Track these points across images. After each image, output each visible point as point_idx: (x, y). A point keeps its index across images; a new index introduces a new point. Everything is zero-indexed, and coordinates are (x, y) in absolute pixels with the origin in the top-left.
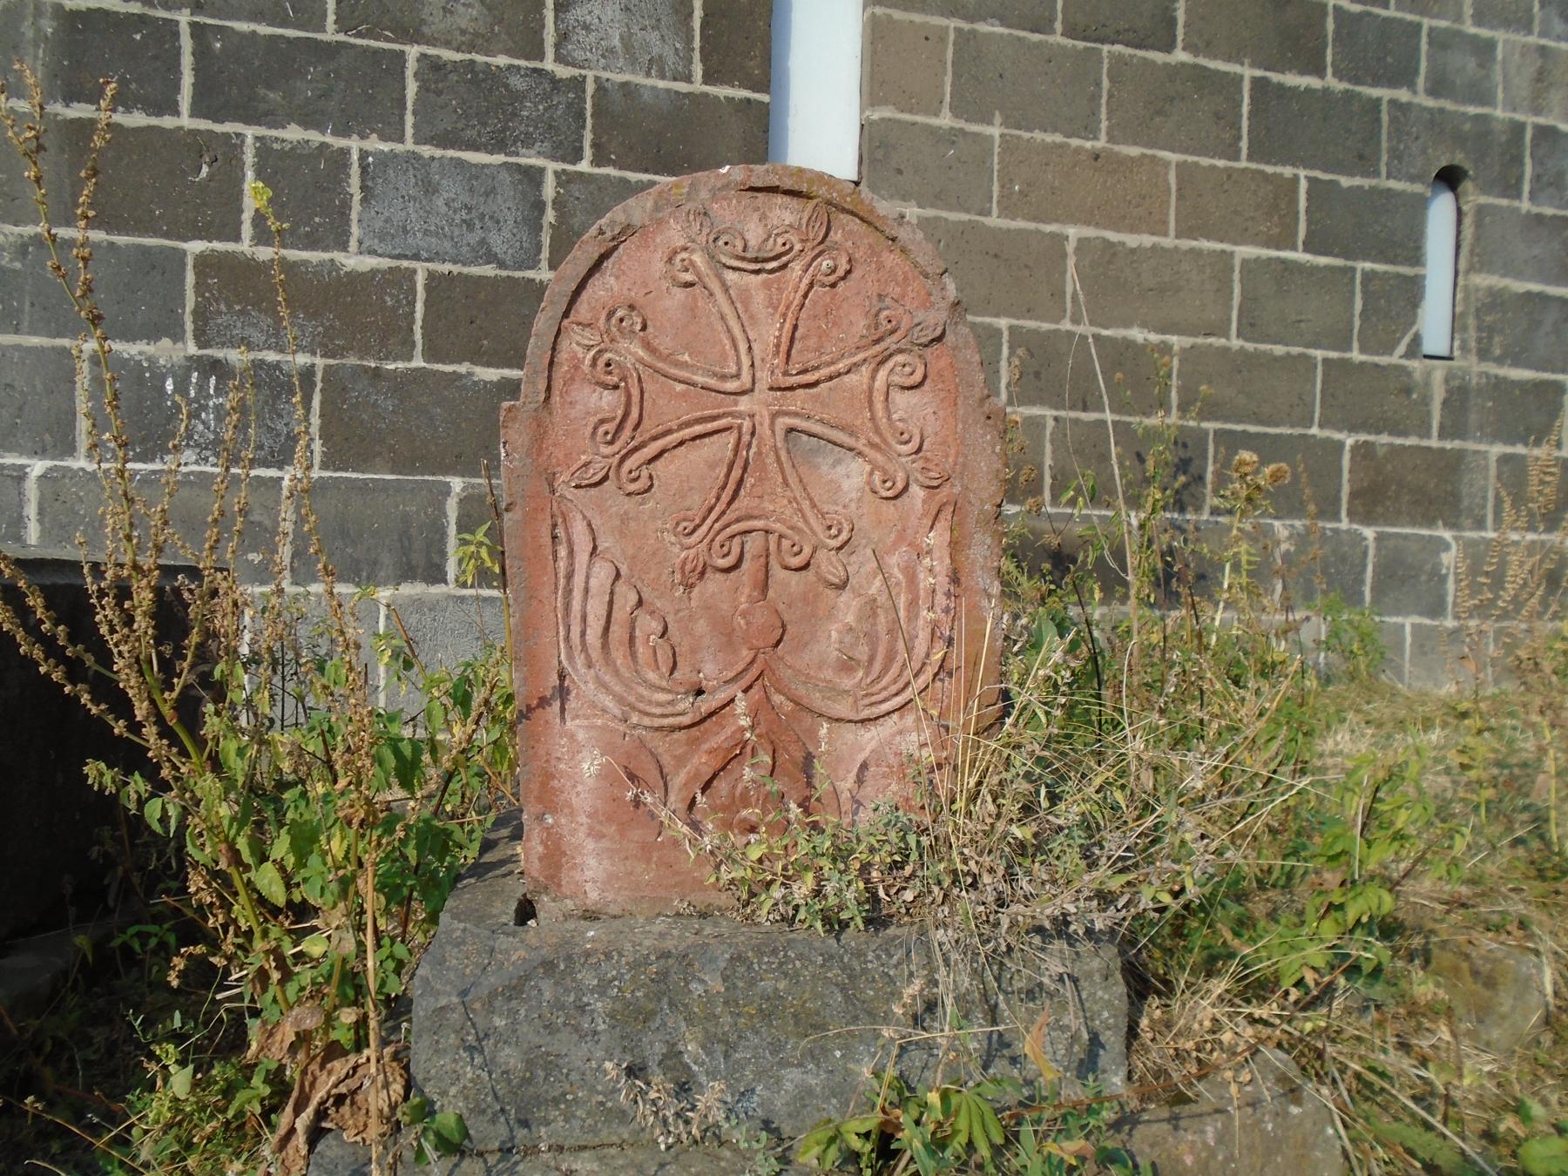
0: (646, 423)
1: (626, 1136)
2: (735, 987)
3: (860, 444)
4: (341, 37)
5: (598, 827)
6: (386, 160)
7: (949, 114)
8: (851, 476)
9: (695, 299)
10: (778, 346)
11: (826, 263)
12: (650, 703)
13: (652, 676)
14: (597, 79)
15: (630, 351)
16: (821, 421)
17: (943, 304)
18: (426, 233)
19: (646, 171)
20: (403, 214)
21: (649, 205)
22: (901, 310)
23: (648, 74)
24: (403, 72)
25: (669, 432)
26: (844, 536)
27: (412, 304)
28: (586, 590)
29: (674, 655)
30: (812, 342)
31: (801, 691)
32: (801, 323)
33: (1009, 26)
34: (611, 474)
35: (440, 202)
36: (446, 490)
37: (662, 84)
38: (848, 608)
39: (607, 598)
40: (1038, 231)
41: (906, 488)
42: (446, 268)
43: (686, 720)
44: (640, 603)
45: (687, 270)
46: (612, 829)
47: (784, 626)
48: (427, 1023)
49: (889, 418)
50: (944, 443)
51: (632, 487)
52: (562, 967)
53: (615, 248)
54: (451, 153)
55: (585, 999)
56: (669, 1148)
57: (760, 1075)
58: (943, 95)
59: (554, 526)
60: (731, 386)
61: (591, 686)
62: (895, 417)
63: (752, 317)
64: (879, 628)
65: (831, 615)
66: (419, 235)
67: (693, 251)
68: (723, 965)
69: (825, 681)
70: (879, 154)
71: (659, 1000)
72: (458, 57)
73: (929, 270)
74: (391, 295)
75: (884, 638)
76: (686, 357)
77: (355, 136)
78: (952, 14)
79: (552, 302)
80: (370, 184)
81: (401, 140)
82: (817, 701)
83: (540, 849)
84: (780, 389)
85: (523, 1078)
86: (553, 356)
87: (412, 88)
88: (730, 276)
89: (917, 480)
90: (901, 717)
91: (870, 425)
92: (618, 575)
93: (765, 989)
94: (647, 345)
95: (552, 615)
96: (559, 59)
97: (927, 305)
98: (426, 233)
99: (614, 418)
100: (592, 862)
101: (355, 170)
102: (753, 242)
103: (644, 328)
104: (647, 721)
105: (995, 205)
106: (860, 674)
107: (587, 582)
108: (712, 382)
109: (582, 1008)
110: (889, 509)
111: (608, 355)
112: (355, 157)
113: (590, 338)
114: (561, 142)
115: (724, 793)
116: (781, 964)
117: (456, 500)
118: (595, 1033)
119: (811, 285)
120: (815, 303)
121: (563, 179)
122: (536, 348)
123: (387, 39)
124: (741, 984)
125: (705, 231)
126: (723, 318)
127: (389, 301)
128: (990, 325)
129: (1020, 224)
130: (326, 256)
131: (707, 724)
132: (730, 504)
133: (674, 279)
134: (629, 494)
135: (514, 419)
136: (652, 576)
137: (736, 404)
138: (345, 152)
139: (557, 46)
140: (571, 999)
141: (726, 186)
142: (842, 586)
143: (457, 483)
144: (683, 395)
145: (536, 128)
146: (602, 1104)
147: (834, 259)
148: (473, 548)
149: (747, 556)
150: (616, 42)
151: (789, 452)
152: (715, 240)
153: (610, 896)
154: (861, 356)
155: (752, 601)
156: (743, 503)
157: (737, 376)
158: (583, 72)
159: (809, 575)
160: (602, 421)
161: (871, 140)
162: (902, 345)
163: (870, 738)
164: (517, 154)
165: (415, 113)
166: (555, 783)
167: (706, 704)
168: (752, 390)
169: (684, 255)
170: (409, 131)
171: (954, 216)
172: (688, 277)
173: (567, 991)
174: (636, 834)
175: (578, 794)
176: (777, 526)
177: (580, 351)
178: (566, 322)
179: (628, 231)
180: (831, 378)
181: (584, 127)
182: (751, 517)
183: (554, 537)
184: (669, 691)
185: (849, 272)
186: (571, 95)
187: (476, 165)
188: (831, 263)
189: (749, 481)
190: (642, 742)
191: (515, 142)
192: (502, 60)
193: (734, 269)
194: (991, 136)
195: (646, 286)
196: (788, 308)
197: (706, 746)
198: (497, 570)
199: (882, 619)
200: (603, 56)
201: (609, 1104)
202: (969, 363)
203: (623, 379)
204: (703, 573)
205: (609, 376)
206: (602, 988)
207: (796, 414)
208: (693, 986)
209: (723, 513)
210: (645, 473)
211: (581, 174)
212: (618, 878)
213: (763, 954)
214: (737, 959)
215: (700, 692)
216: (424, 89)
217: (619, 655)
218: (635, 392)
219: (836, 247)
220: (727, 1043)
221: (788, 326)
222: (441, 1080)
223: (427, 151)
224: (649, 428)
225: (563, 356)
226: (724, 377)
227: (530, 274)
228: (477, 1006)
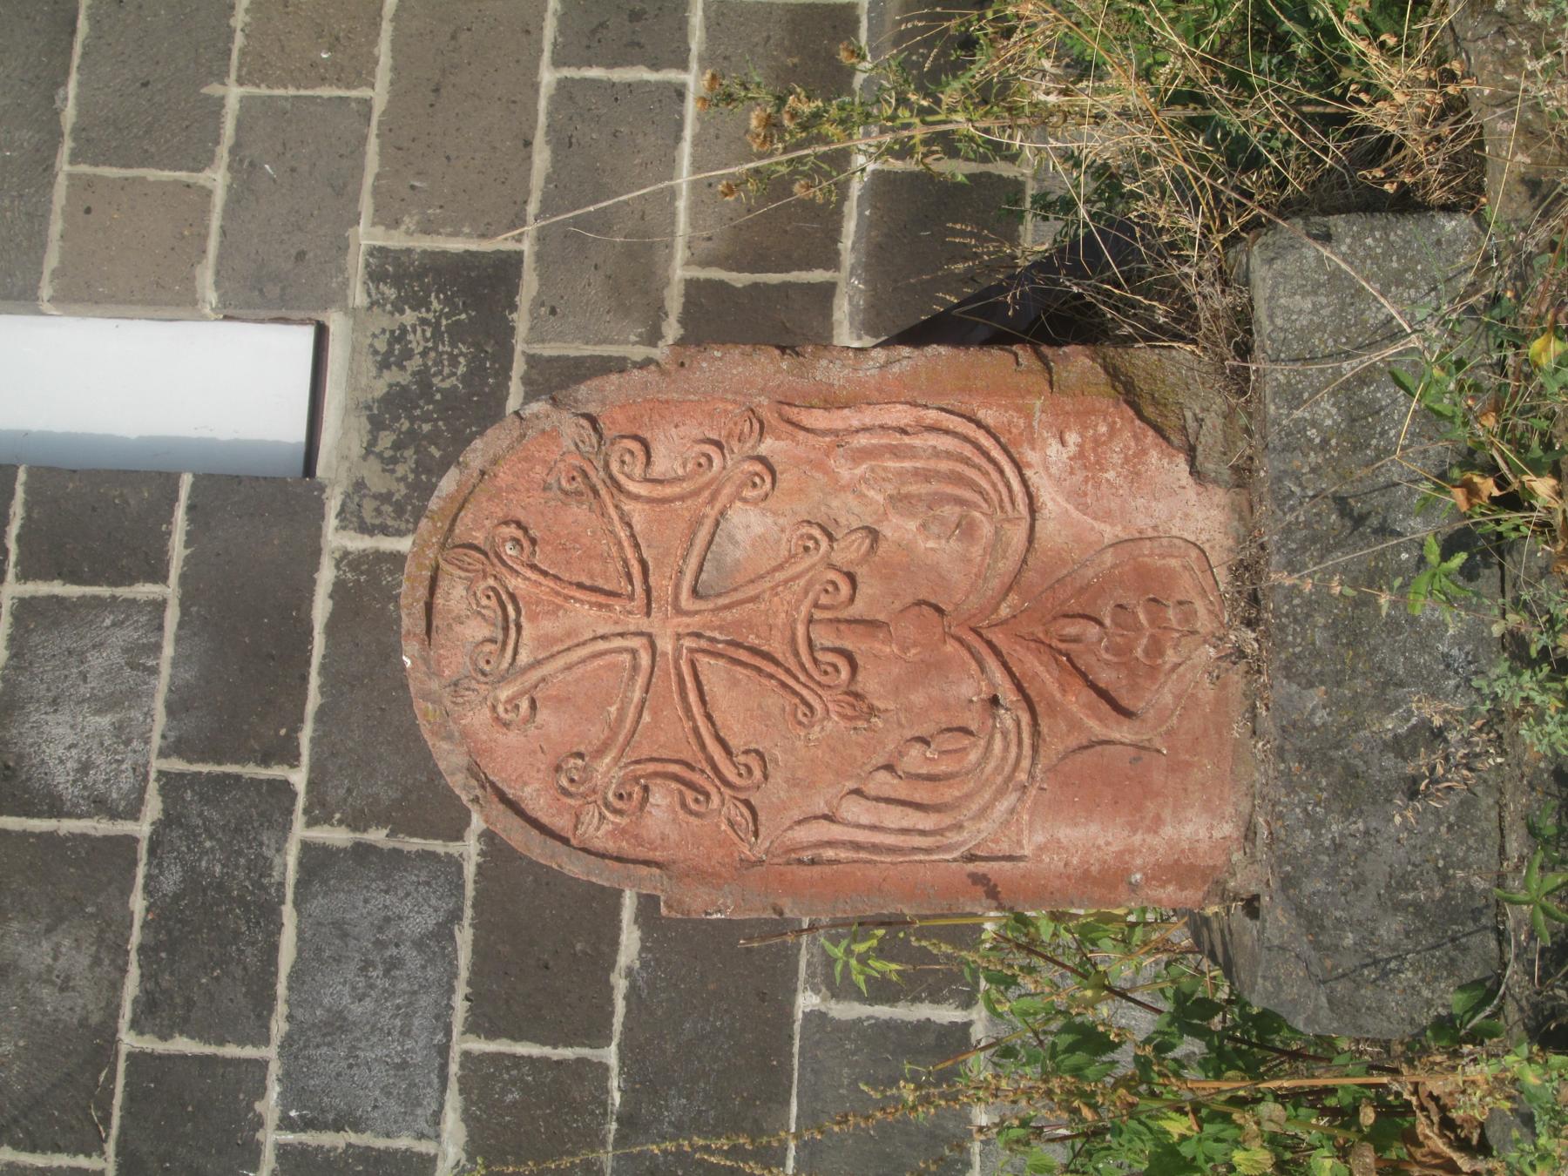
0: (684, 756)
1: (1491, 801)
2: (1321, 673)
3: (712, 512)
4: (110, 1147)
5: (1147, 822)
6: (294, 1091)
7: (208, 173)
8: (749, 525)
9: (548, 698)
10: (600, 606)
11: (509, 550)
12: (1004, 759)
13: (973, 756)
14: (163, 754)
16: (684, 558)
17: (555, 416)
18: (406, 1033)
19: (305, 679)
20: (376, 1068)
21: (445, 746)
22: (561, 465)
23: (154, 671)
24: (160, 1057)
25: (696, 730)
26: (817, 533)
27: (517, 1060)
28: (873, 828)
29: (949, 730)
30: (597, 567)
31: (995, 583)
32: (575, 579)
33: (67, 73)
34: (742, 796)
35: (357, 1009)
36: (816, 1019)
37: (168, 650)
38: (900, 528)
39: (883, 805)
40: (396, 18)
41: (762, 460)
42: (460, 1005)
43: (1025, 718)
44: (889, 768)
45: (517, 707)
46: (1151, 806)
47: (920, 603)
48: (1347, 1019)
49: (680, 479)
50: (711, 415)
51: (757, 773)
52: (1289, 868)
53: (493, 785)
54: (281, 989)
55: (1327, 843)
56: (1503, 753)
57: (1424, 646)
58: (176, 182)
59: (800, 862)
60: (645, 659)
61: (983, 825)
62: (680, 472)
63: (569, 635)
64: (923, 491)
65: (906, 548)
66: (409, 1044)
67: (496, 699)
68: (1294, 687)
69: (984, 555)
70: (273, 291)
71: (1332, 760)
72: (134, 972)
73: (516, 434)
74: (504, 1092)
75: (935, 486)
76: (613, 709)
77: (259, 1135)
78: (49, 168)
79: (552, 857)
80: (331, 1117)
81: (263, 1065)
82: (1007, 565)
83: (1171, 888)
84: (649, 604)
85: (1415, 914)
86: (611, 858)
88: (524, 657)
89: (753, 447)
90: (1030, 465)
91: (689, 502)
92: (857, 792)
93: (1325, 640)
94: (600, 752)
95: (900, 868)
96: (133, 813)
97: (553, 435)
98: (406, 1033)
99: (680, 792)
100: (1188, 830)
101: (310, 1138)
102: (484, 631)
103: (580, 755)
104: (1026, 763)
105: (353, 93)
106: (977, 514)
107: (863, 827)
108: (641, 680)
109: (1338, 847)
110: (786, 480)
111: (610, 797)
112: (289, 1137)
113: (591, 816)
114: (262, 814)
115: (1114, 675)
116: (1296, 621)
117: (832, 1004)
118: (1367, 833)
119: (533, 567)
120: (553, 564)
122: (602, 875)
123: (112, 1077)
124: (1318, 667)
125: (474, 685)
126: (569, 667)
127: (513, 1096)
128: (552, 100)
129: (384, 50)
131: (1032, 693)
132: (777, 663)
133: (526, 721)
134: (766, 777)
135: (680, 902)
136: (858, 753)
137: (665, 654)
138: (283, 1151)
139: (114, 815)
140: (1326, 859)
141: (426, 661)
142: (874, 534)
143: (807, 1001)
144: (655, 713)
145: (240, 853)
146: (1450, 827)
147: (504, 541)
148: (853, 962)
149: (838, 644)
150: (105, 721)
151: (719, 595)
152: (484, 674)
153: (1229, 810)
154: (612, 511)
155: (889, 639)
156: (777, 648)
157: (634, 652)
158: (153, 775)
159: (861, 572)
160: (684, 805)
161: (249, 305)
162: (600, 464)
163: (1052, 500)
164: (281, 884)
165: (221, 1042)
166: (1094, 869)
167: (1008, 695)
168: (650, 636)
169: (501, 709)
170: (249, 1052)
172: (524, 705)
173: (1316, 863)
174: (1158, 778)
175: (1108, 844)
176: (804, 609)
177: (606, 827)
178: (574, 842)
179: (474, 771)
180: (637, 546)
181: (238, 777)
182: (793, 640)
183: (813, 862)
184: (992, 737)
185: (519, 525)
186: (189, 795)
187: (300, 951)
188: (509, 545)
189: (752, 640)
190: (1051, 769)
191: (263, 888)
192: (138, 903)
193: (516, 652)
194: (242, 100)
195: (535, 752)
196: (558, 594)
197: (1058, 695)
198: (881, 932)
199: (913, 489)
200: (128, 742)
201: (1452, 819)
202: (620, 386)
203: (636, 779)
204: (857, 695)
205: (632, 796)
206: (1315, 824)
207: (677, 587)
208: (1317, 721)
209: (788, 671)
210: (742, 759)
211: (311, 783)
212: (1209, 800)
213: (1284, 642)
214: (1288, 670)
215: (994, 701)
217: (949, 793)
218: (651, 767)
219: (491, 539)
220: (1386, 684)
221: (578, 594)
222: (1414, 1006)
223: (279, 1026)
224: (690, 752)
225: (611, 846)
226: (635, 668)
227: (470, 871)
228: (1328, 963)
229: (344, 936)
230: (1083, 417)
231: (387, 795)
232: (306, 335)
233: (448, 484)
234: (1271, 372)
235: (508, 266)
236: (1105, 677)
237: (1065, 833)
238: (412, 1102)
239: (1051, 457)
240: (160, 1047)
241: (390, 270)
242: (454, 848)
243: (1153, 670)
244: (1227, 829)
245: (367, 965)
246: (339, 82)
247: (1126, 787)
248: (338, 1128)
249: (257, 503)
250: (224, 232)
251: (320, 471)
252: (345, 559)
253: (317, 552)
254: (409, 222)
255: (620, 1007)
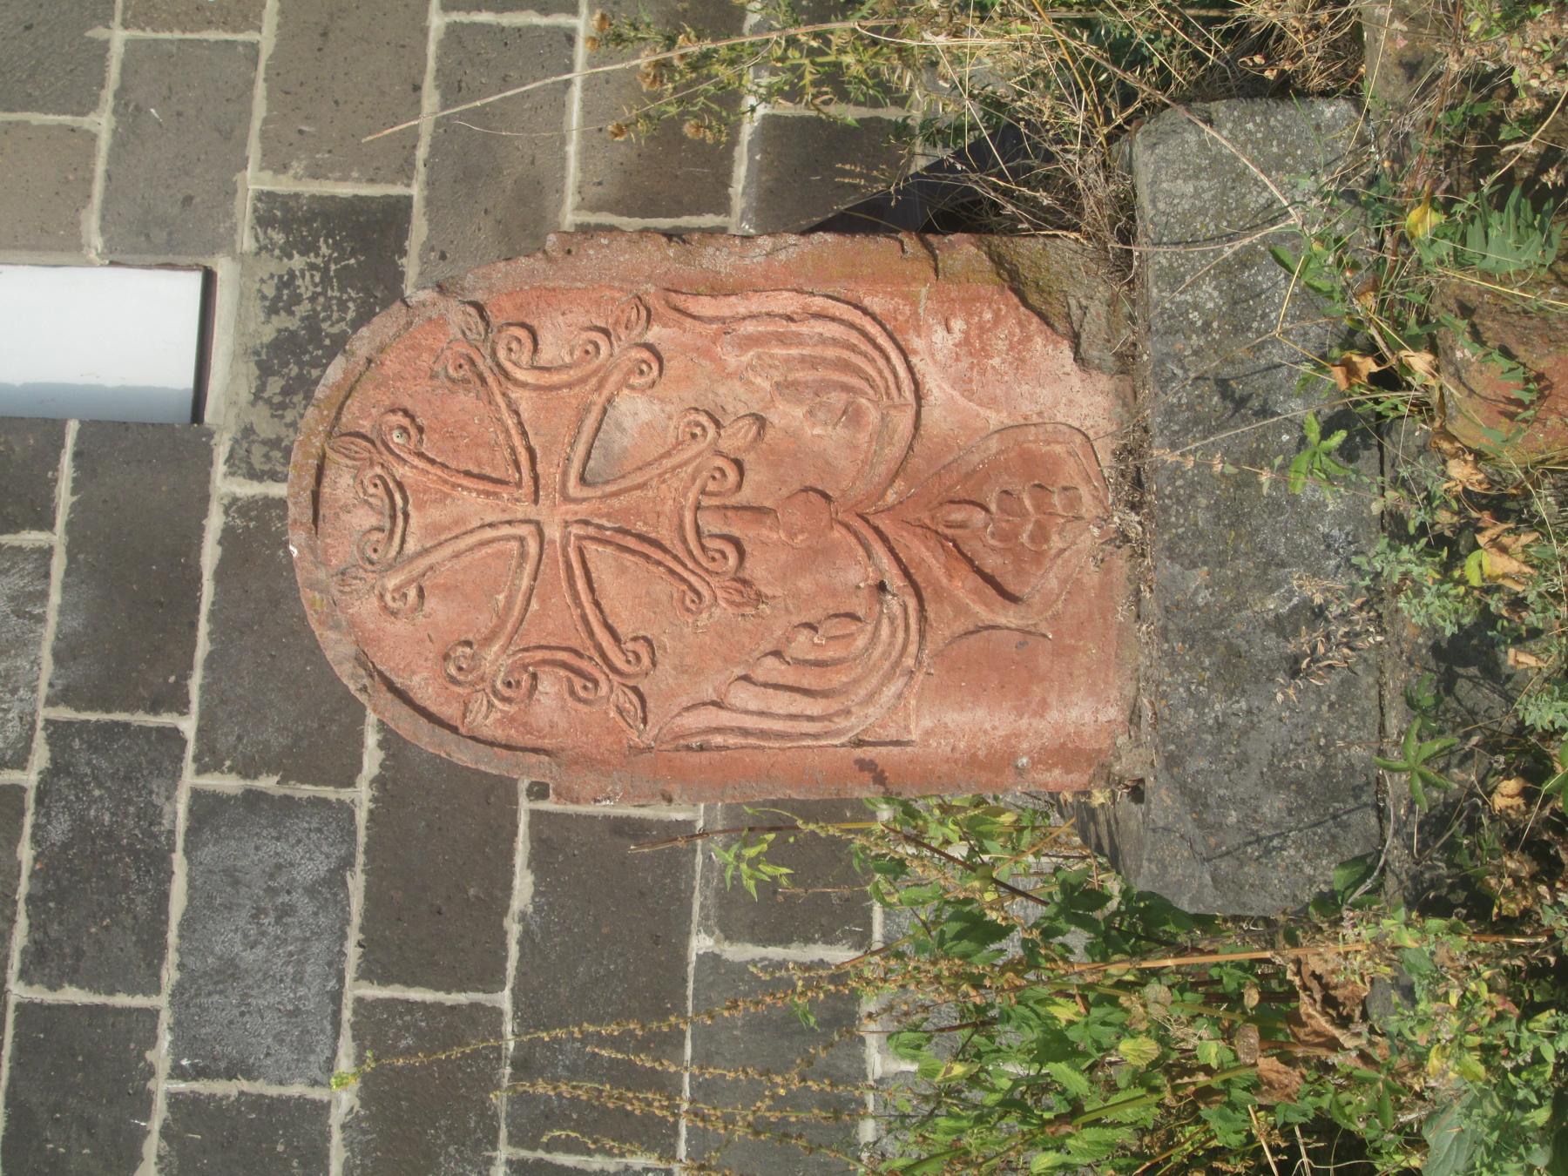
0: (574, 643)
1: (1371, 680)
2: (1203, 554)
3: (599, 400)
5: (1034, 706)
6: (185, 1040)
7: (92, 117)
8: (636, 412)
9: (437, 586)
10: (488, 494)
11: (396, 438)
12: (891, 644)
13: (861, 642)
14: (50, 702)
15: (494, 659)
16: (572, 445)
17: (441, 304)
18: (298, 979)
19: (193, 625)
20: (268, 1015)
21: (332, 635)
22: (448, 353)
23: (41, 619)
24: (50, 1007)
25: (584, 618)
26: (704, 419)
27: (410, 1006)
28: (761, 714)
29: (836, 616)
30: (484, 454)
31: (882, 469)
32: (463, 467)
34: (631, 683)
35: (249, 956)
36: (711, 961)
37: (55, 598)
38: (787, 415)
39: (771, 691)
41: (649, 347)
42: (353, 952)
43: (912, 604)
44: (777, 654)
45: (405, 595)
46: (1037, 690)
47: (806, 490)
48: (1231, 896)
49: (568, 367)
50: (598, 303)
51: (646, 660)
52: (1172, 747)
53: (381, 674)
54: (172, 937)
55: (1211, 722)
56: (1383, 632)
57: (1306, 528)
58: (60, 126)
59: (688, 748)
60: (533, 547)
61: (871, 710)
62: (568, 359)
63: (456, 523)
64: (810, 378)
65: (792, 435)
66: (302, 991)
67: (384, 588)
68: (1178, 567)
69: (870, 442)
70: (160, 236)
71: (1215, 640)
73: (402, 322)
74: (397, 1038)
75: (821, 373)
76: (501, 597)
77: (151, 1085)
79: (440, 745)
80: (223, 1065)
81: (153, 1014)
82: (894, 451)
83: (1057, 772)
84: (536, 492)
85: (1297, 792)
86: (500, 746)
87: (72, 995)
88: (412, 546)
89: (641, 335)
90: (915, 352)
91: (577, 390)
92: (746, 678)
93: (1207, 521)
94: (488, 641)
95: (788, 753)
96: (20, 762)
97: (440, 323)
98: (298, 979)
99: (569, 679)
100: (1074, 713)
101: (202, 1087)
102: (371, 520)
103: (469, 644)
104: (913, 649)
105: (240, 37)
106: (863, 401)
107: (752, 713)
108: (529, 568)
109: (1221, 726)
110: (674, 366)
111: (499, 685)
112: (181, 1086)
113: (479, 705)
114: (151, 762)
115: (1000, 561)
116: (1179, 502)
117: (726, 946)
118: (1249, 712)
119: (421, 455)
120: (441, 451)
121: (209, 760)
122: (491, 764)
124: (1201, 548)
125: (361, 573)
126: (457, 555)
128: (442, 44)
130: (337, 1137)
131: (919, 579)
132: (665, 550)
133: (414, 610)
134: (654, 664)
135: (569, 789)
136: (746, 640)
137: (553, 542)
138: (175, 1101)
140: (1210, 738)
141: (313, 550)
142: (761, 421)
143: (700, 943)
144: (543, 602)
145: (129, 802)
146: (1331, 706)
147: (391, 429)
148: (744, 866)
149: (726, 530)
151: (607, 482)
152: (371, 563)
153: (1114, 694)
154: (499, 399)
155: (776, 526)
156: (665, 535)
157: (521, 540)
158: (40, 724)
159: (749, 459)
160: (572, 693)
161: (135, 250)
162: (487, 352)
163: (936, 386)
164: (172, 832)
165: (111, 992)
166: (981, 754)
167: (895, 580)
168: (537, 524)
169: (388, 597)
170: (140, 1001)
171: (260, 108)
172: (412, 593)
173: (1200, 741)
174: (1044, 662)
175: (994, 728)
176: (691, 496)
177: (495, 716)
178: (463, 730)
179: (362, 660)
180: (524, 434)
181: (127, 725)
182: (681, 527)
183: (701, 748)
184: (879, 622)
185: (406, 413)
186: (77, 744)
187: (191, 899)
188: (396, 433)
189: (640, 527)
190: (939, 655)
191: (154, 836)
192: (26, 853)
193: (403, 541)
194: (127, 43)
195: (423, 641)
196: (445, 482)
197: (944, 581)
198: (771, 836)
199: (800, 375)
200: (14, 691)
201: (1333, 697)
202: (507, 275)
203: (525, 667)
204: (744, 582)
205: (521, 683)
206: (1199, 703)
207: (565, 474)
208: (1200, 601)
209: (676, 558)
210: (630, 646)
211: (201, 731)
212: (1094, 684)
213: (1167, 523)
214: (1171, 551)
215: (882, 587)
216: (73, 976)
217: (837, 679)
218: (539, 655)
219: (378, 427)
220: (1268, 564)
221: (466, 482)
222: (1296, 883)
223: (170, 975)
224: (579, 640)
225: (500, 735)
226: (523, 555)
227: (361, 817)
228: (1212, 841)
229: (236, 883)
230: (968, 304)
231: (278, 741)
232: (191, 283)
233: (335, 371)
234: (1152, 255)
235: (398, 211)
236: (991, 563)
237: (952, 718)
238: (304, 1048)
239: (937, 344)
240: (50, 997)
241: (279, 215)
242: (345, 794)
243: (1038, 557)
244: (1112, 713)
245: (259, 912)
246: (225, 25)
247: (1011, 670)
248: (230, 1075)
249: (146, 450)
250: (109, 177)
251: (208, 417)
252: (234, 505)
253: (206, 499)
254: (297, 167)
255: (514, 951)
